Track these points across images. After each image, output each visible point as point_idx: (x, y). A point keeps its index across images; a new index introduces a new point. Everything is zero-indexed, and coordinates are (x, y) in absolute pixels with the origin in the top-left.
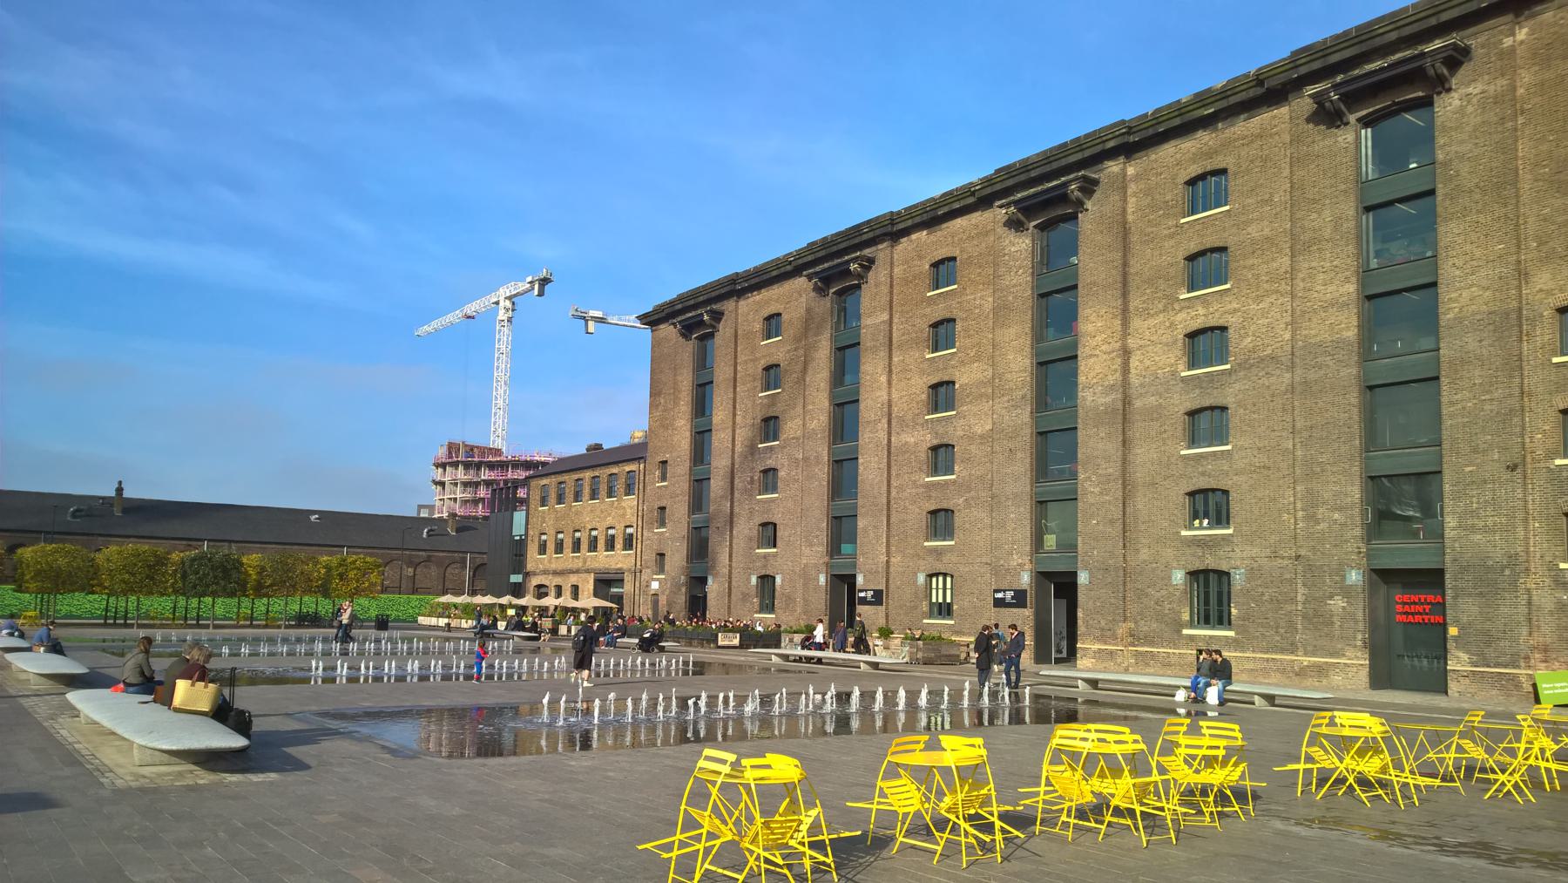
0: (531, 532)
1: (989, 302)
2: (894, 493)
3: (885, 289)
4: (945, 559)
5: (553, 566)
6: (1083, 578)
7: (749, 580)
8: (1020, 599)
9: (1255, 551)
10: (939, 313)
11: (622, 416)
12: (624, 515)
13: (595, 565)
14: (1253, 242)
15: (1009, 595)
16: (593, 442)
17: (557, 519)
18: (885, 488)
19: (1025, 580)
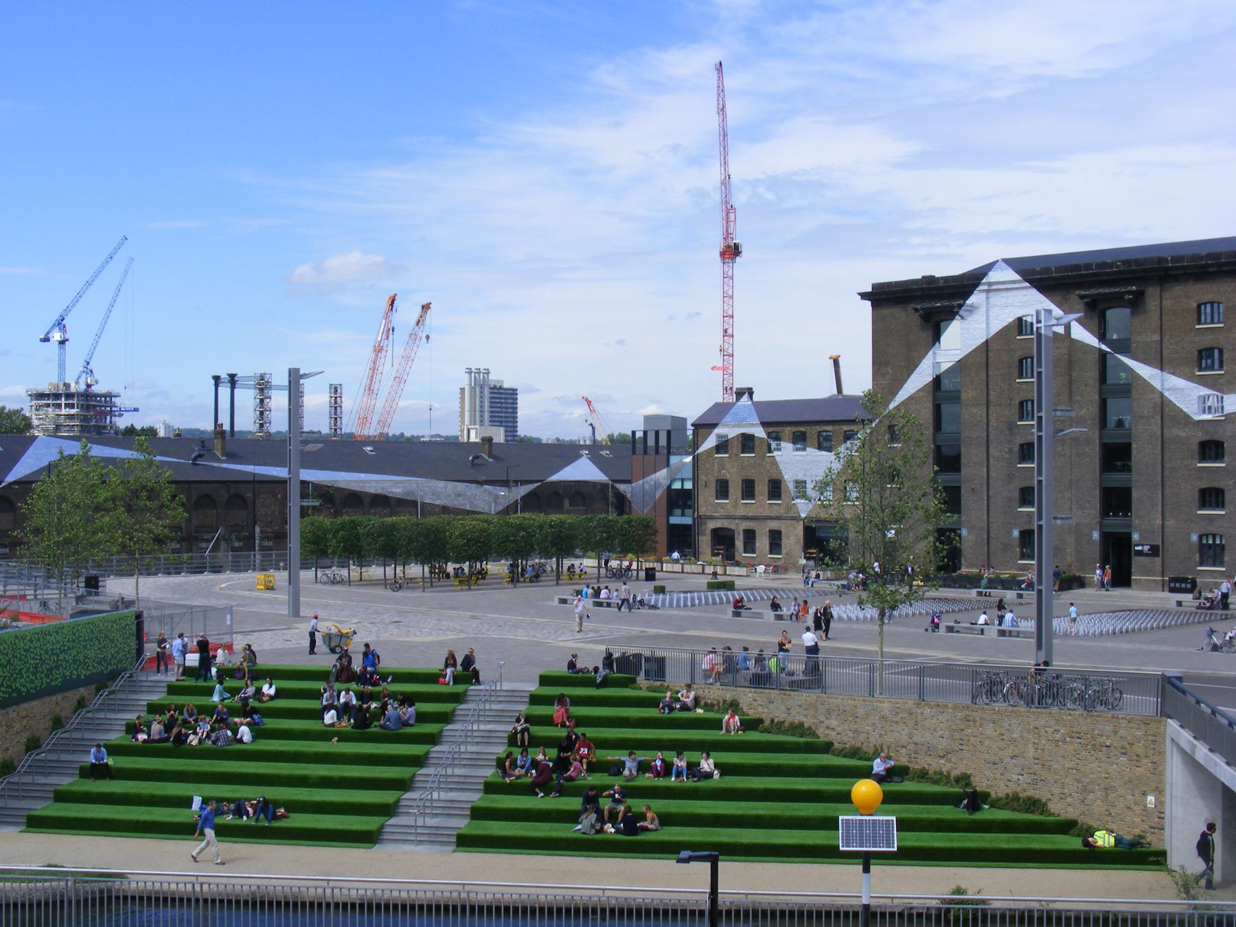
2: (1167, 473)
3: (1156, 317)
5: (741, 512)
7: (1010, 533)
10: (1207, 341)
18: (1159, 469)
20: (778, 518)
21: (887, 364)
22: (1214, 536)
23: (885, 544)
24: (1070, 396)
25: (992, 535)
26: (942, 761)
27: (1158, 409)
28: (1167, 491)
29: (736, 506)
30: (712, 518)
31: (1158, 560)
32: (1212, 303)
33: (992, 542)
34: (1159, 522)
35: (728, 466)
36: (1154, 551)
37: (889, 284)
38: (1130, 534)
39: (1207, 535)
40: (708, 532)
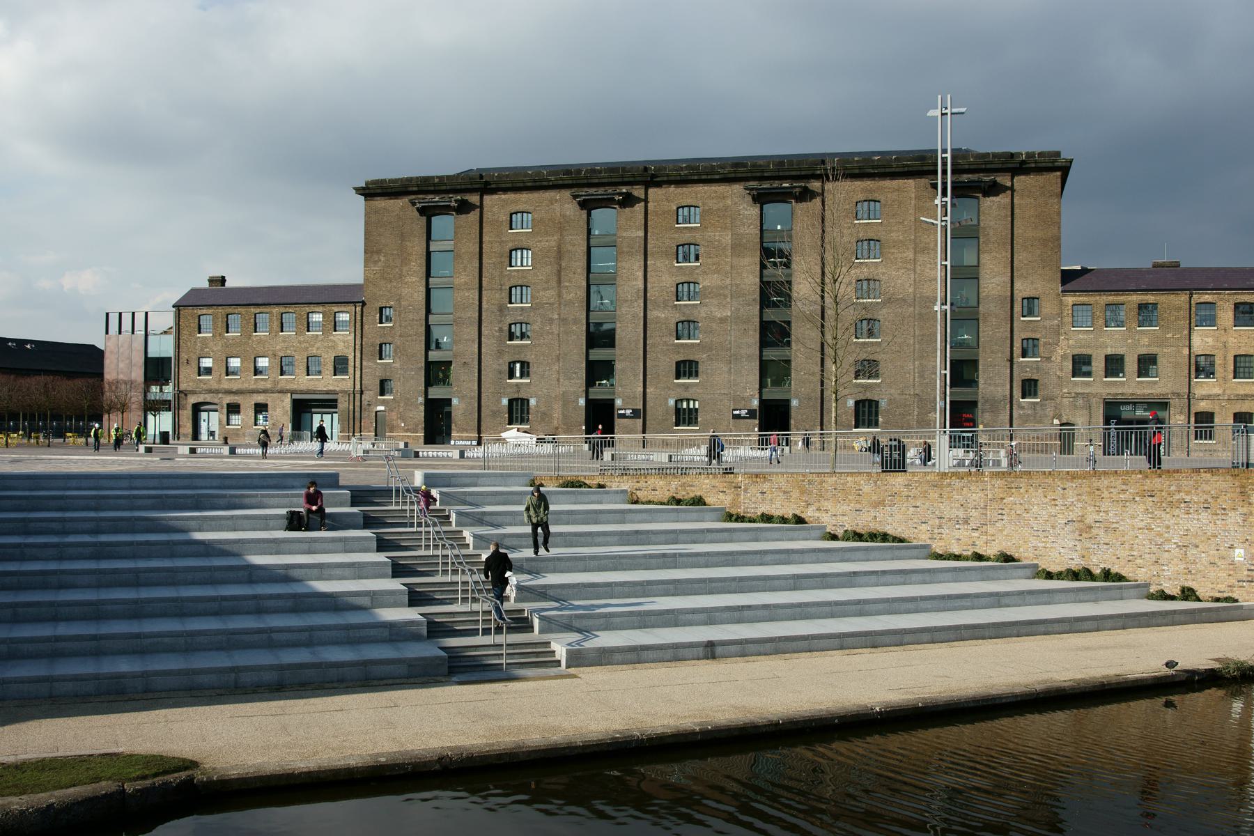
0: (184, 356)
1: (727, 239)
4: (692, 390)
5: (226, 386)
6: (794, 403)
7: (499, 401)
9: (893, 391)
10: (686, 238)
11: (344, 266)
12: (334, 347)
14: (894, 241)
15: (744, 412)
16: (218, 273)
19: (755, 403)
20: (265, 391)
21: (379, 252)
22: (688, 400)
24: (559, 282)
26: (976, 534)
27: (642, 294)
29: (219, 381)
30: (194, 393)
32: (689, 206)
34: (641, 389)
35: (211, 344)
36: (636, 414)
37: (383, 181)
38: (613, 400)
39: (682, 400)
40: (189, 407)
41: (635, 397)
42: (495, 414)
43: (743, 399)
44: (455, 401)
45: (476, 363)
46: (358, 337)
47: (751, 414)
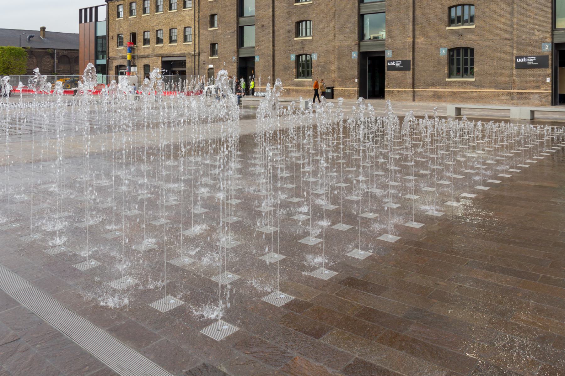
0: (111, 34)
4: (466, 38)
7: (289, 58)
8: (541, 62)
12: (183, 21)
13: (162, 52)
15: (531, 60)
17: (130, 25)
19: (547, 49)
23: (96, 38)
25: (276, 60)
28: (417, 12)
31: (409, 74)
33: (276, 65)
34: (410, 40)
35: (123, 25)
36: (406, 66)
38: (384, 52)
40: (114, 68)
41: (404, 48)
42: (286, 69)
43: (530, 44)
44: (257, 59)
45: (271, 25)
46: (197, 11)
47: (541, 62)
